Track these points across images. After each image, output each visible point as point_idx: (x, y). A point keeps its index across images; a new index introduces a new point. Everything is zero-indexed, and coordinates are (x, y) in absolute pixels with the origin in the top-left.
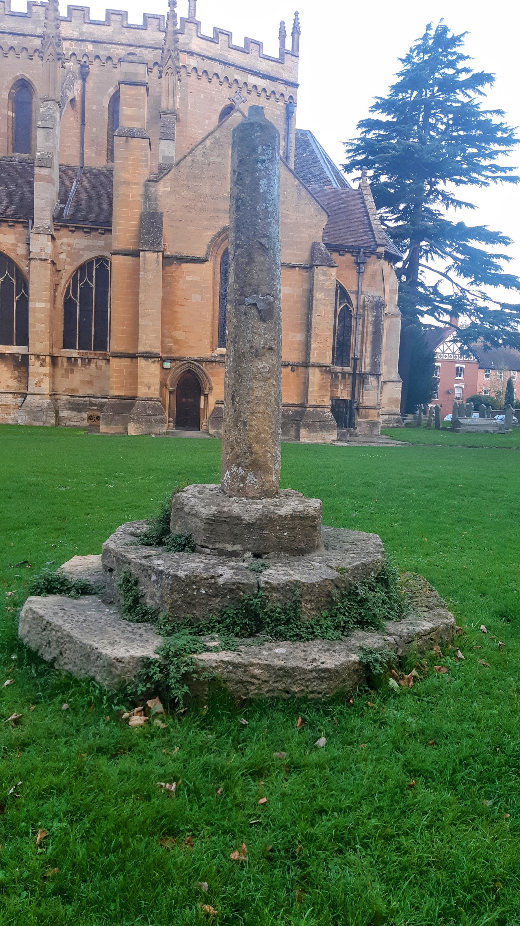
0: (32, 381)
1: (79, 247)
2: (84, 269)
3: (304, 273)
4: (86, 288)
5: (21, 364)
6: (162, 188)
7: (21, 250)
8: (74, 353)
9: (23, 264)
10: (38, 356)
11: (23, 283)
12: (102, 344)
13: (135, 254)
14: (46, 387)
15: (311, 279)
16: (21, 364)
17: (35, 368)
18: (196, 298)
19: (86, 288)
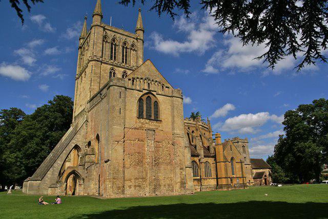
6: (225, 152)
7: (198, 161)
9: (198, 163)
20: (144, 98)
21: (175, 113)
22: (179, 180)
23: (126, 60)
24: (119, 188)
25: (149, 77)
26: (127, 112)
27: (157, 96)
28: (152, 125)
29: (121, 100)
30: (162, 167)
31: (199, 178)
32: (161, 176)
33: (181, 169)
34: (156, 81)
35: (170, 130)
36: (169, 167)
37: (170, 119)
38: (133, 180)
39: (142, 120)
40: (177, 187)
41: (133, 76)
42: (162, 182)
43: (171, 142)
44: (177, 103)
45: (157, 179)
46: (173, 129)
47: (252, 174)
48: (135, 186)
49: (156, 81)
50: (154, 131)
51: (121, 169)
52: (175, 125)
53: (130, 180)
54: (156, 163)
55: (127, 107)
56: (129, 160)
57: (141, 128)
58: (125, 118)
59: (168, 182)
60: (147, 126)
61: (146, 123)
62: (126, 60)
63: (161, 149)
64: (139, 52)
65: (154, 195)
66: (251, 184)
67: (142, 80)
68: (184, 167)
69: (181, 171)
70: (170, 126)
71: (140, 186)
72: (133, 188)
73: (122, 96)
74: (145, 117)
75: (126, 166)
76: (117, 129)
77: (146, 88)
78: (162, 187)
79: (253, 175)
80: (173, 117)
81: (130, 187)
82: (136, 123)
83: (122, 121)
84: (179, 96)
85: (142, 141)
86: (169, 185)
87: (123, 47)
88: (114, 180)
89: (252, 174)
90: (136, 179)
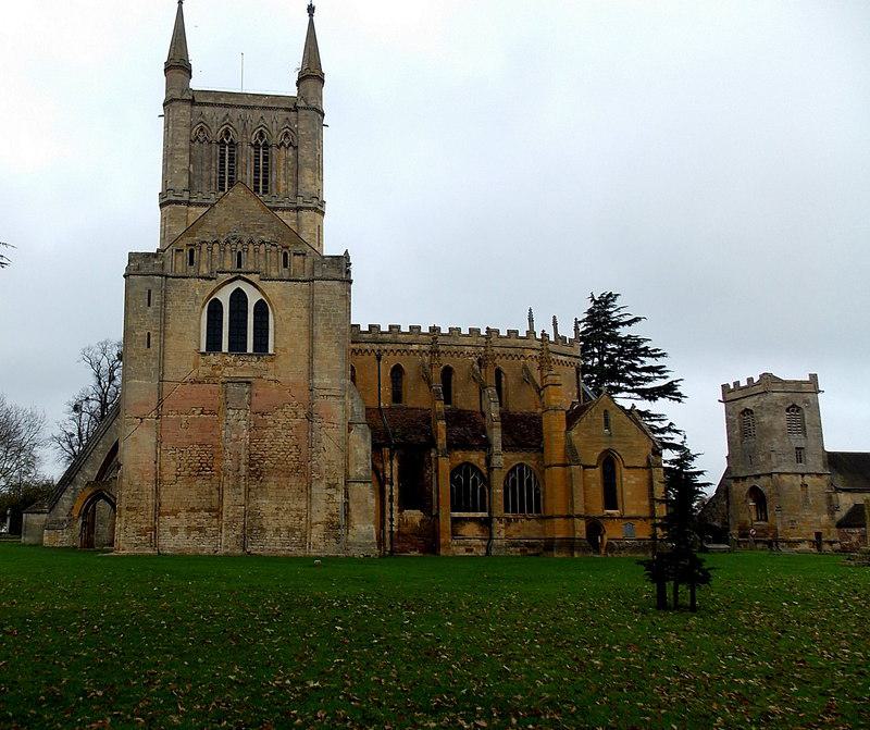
0: (495, 532)
1: (515, 458)
2: (513, 470)
3: (646, 472)
4: (514, 481)
5: (486, 524)
6: (573, 433)
7: (483, 462)
8: (510, 515)
10: (498, 518)
11: (487, 482)
12: (538, 511)
13: (564, 465)
14: (503, 534)
15: (651, 472)
16: (486, 524)
17: (498, 526)
18: (593, 485)
19: (514, 481)
20: (224, 297)
21: (319, 329)
22: (320, 516)
23: (265, 182)
24: (141, 532)
25: (240, 233)
26: (170, 341)
27: (261, 284)
28: (245, 367)
29: (150, 310)
30: (272, 482)
31: (485, 514)
32: (266, 505)
33: (330, 486)
34: (263, 242)
35: (303, 379)
36: (293, 481)
37: (303, 347)
38: (183, 515)
39: (214, 358)
40: (316, 534)
41: (189, 240)
42: (270, 523)
43: (302, 413)
44: (326, 298)
45: (252, 514)
46: (311, 375)
47: (833, 509)
48: (189, 529)
49: (263, 242)
50: (248, 383)
51: (151, 486)
52: (316, 362)
53: (175, 513)
54: (256, 472)
55: (169, 328)
56: (174, 464)
57: (209, 379)
58: (162, 357)
59: (288, 520)
60: (228, 372)
61: (227, 365)
62: (265, 182)
63: (270, 433)
64: (302, 151)
65: (239, 551)
66: (826, 547)
67: (216, 248)
68: (342, 482)
69: (329, 491)
70: (302, 366)
71: (201, 530)
72: (182, 534)
73: (155, 299)
74: (225, 348)
75: (166, 478)
76: (140, 386)
77: (229, 264)
78: (269, 534)
79: (839, 516)
80: (312, 338)
81: (174, 530)
82: (196, 365)
83: (155, 364)
84: (336, 275)
85: (213, 413)
86: (291, 530)
87: (256, 146)
88: (131, 513)
89: (833, 509)
90: (193, 510)
